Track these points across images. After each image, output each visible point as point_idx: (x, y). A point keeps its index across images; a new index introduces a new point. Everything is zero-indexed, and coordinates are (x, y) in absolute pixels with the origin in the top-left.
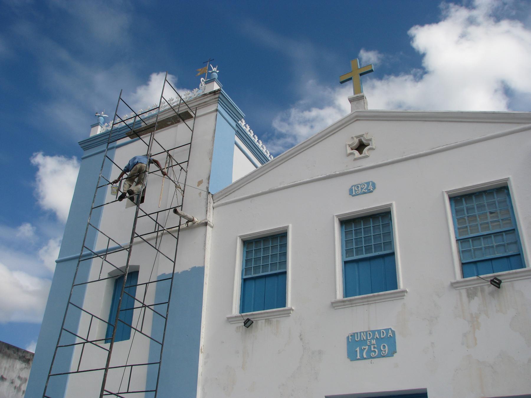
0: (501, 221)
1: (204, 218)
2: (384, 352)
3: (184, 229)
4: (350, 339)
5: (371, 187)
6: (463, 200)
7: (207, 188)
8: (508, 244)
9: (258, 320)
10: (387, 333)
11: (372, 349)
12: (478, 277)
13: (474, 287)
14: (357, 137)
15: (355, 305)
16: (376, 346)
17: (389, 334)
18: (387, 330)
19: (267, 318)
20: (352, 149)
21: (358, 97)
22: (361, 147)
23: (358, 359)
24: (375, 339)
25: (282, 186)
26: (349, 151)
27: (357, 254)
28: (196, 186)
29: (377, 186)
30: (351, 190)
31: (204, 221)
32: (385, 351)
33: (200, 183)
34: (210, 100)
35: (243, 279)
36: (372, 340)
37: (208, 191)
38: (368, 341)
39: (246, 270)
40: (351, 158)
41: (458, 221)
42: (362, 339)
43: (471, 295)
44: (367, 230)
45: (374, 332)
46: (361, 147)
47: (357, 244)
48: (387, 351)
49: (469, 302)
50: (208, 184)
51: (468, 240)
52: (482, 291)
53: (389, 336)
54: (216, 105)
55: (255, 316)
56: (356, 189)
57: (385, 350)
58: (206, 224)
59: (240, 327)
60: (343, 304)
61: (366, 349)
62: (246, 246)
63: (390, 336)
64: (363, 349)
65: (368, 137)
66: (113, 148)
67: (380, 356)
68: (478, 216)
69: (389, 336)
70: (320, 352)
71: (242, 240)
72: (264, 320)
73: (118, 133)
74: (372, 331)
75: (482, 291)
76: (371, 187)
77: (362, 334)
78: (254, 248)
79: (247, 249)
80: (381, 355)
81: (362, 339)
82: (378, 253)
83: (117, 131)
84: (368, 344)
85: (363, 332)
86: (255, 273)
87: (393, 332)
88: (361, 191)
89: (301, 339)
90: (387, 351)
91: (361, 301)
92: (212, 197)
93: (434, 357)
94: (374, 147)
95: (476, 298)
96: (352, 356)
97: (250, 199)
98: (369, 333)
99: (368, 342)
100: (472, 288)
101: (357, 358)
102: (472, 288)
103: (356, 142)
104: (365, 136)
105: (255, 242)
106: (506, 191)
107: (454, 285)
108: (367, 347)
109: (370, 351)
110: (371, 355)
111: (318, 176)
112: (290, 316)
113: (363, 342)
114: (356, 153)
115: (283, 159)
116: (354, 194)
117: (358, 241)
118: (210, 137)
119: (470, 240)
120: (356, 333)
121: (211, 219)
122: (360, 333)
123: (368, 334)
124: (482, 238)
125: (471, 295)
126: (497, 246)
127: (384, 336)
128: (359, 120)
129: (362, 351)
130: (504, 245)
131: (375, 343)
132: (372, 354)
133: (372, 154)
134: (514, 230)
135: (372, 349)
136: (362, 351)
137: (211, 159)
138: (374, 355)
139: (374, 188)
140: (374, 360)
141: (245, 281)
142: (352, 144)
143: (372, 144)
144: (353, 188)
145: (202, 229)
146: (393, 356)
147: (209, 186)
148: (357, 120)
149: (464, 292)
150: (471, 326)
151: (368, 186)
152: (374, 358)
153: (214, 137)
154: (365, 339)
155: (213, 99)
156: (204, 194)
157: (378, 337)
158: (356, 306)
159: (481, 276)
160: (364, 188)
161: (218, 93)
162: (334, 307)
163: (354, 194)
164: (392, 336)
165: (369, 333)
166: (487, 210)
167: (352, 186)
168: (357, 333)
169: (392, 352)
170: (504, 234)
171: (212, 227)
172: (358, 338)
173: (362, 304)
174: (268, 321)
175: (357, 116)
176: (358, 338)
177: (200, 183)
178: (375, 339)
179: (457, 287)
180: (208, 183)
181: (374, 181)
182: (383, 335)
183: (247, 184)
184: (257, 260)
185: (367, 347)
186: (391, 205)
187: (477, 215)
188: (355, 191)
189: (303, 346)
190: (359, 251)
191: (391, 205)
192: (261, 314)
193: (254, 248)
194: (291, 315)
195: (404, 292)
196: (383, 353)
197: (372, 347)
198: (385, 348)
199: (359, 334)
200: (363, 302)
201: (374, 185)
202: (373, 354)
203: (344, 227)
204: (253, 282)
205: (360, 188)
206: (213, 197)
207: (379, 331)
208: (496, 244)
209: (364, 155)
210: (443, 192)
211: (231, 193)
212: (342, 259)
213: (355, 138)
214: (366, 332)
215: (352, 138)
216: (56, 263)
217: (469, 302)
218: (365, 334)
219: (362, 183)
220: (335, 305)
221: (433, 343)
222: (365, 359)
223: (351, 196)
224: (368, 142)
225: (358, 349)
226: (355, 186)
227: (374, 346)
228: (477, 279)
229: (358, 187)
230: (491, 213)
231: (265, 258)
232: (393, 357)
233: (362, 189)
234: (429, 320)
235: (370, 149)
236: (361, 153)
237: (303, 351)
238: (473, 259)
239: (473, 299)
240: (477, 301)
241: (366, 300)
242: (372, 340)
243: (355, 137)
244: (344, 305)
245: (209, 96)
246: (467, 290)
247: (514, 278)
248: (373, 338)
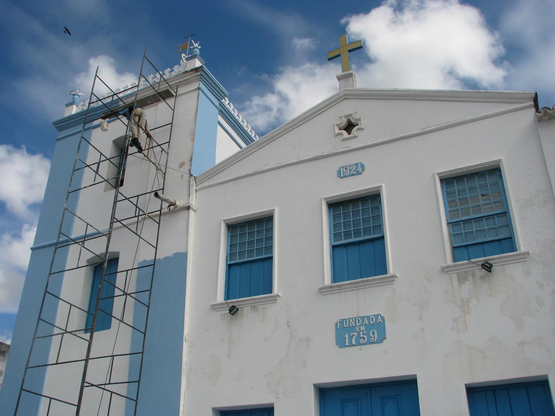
0: (492, 204)
1: (186, 202)
2: (373, 339)
3: (166, 213)
4: (338, 326)
5: (360, 169)
7: (190, 171)
8: (499, 227)
9: (244, 307)
10: (377, 319)
11: (362, 336)
12: (469, 261)
13: (465, 272)
14: (345, 117)
15: (343, 291)
16: (365, 332)
17: (379, 320)
18: (376, 316)
19: (253, 305)
20: (340, 129)
21: (346, 74)
22: (349, 127)
23: (347, 346)
24: (364, 325)
25: (268, 168)
26: (337, 131)
27: (345, 238)
28: (178, 169)
29: (366, 168)
30: (339, 172)
31: (186, 205)
32: (374, 337)
33: (182, 165)
34: (192, 78)
35: (228, 265)
36: (361, 327)
38: (357, 327)
39: (231, 255)
40: (340, 138)
41: (449, 204)
42: (351, 326)
43: (462, 280)
44: (356, 214)
45: (363, 318)
46: (349, 127)
47: (345, 227)
48: (376, 338)
49: (460, 286)
51: (459, 223)
52: (473, 275)
53: (378, 322)
54: (199, 82)
55: (240, 303)
56: (344, 171)
57: (374, 336)
58: (188, 208)
59: (225, 314)
60: (330, 289)
61: (354, 335)
62: (230, 231)
63: (379, 321)
64: (352, 335)
65: (356, 117)
66: (89, 128)
67: (370, 343)
68: (470, 198)
69: (378, 322)
70: (308, 339)
71: (226, 224)
72: (250, 307)
73: (94, 113)
74: (361, 317)
75: (473, 275)
76: (360, 169)
77: (351, 320)
78: (239, 233)
79: (232, 233)
80: (371, 342)
81: (351, 326)
82: (367, 236)
83: (94, 111)
84: (357, 331)
85: (352, 319)
87: (383, 318)
88: (350, 172)
89: (288, 326)
90: (376, 338)
91: (350, 286)
92: (195, 179)
93: (424, 343)
94: (363, 127)
95: (466, 282)
96: (341, 343)
97: (234, 182)
98: (358, 319)
99: (357, 329)
100: (463, 273)
101: (346, 345)
102: (463, 273)
103: (344, 121)
104: (354, 115)
105: (240, 226)
106: (498, 173)
107: (445, 270)
108: (356, 334)
109: (359, 337)
110: (360, 342)
111: (305, 157)
112: (277, 302)
113: (352, 329)
114: (345, 133)
115: (268, 140)
116: (342, 175)
117: (346, 225)
118: (192, 117)
119: (462, 223)
120: (344, 319)
121: (193, 202)
122: (349, 319)
123: (357, 320)
124: (473, 221)
125: (462, 280)
126: (488, 229)
127: (373, 323)
128: (348, 99)
129: (351, 337)
130: (495, 229)
131: (364, 330)
132: (361, 341)
133: (360, 134)
134: (506, 212)
135: (362, 336)
136: (351, 337)
137: (193, 140)
138: (363, 342)
139: (363, 169)
140: (363, 347)
141: (229, 267)
142: (340, 123)
143: (361, 123)
144: (342, 169)
145: (185, 213)
146: (383, 342)
147: (191, 168)
148: (346, 99)
149: (454, 277)
150: (461, 311)
151: (357, 167)
152: (363, 344)
153: (196, 116)
154: (354, 325)
155: (194, 77)
156: (186, 176)
157: (367, 323)
158: (345, 291)
159: (472, 260)
160: (353, 169)
161: (200, 71)
162: (322, 293)
163: (342, 175)
164: (381, 322)
166: (479, 193)
167: (340, 168)
168: (346, 320)
169: (382, 339)
170: (496, 217)
171: (195, 211)
172: (346, 325)
173: (351, 289)
174: (254, 308)
175: (345, 95)
176: (346, 325)
177: (182, 165)
178: (364, 325)
179: (448, 272)
180: (191, 165)
181: (362, 162)
182: (372, 321)
183: (231, 165)
184: (242, 244)
185: (356, 334)
186: (380, 187)
187: (469, 198)
188: (344, 172)
189: (290, 333)
190: (347, 235)
191: (380, 187)
192: (247, 300)
193: (239, 233)
194: (277, 301)
195: (394, 276)
196: (372, 339)
197: (361, 333)
198: (375, 334)
199: (348, 320)
200: (352, 288)
202: (363, 340)
203: (332, 210)
204: (239, 268)
205: (348, 169)
206: (196, 180)
207: (368, 317)
208: (487, 228)
209: (353, 135)
210: (434, 173)
211: (214, 175)
212: (330, 243)
213: (343, 118)
214: (355, 318)
215: (341, 117)
216: (31, 251)
217: (460, 286)
218: (354, 320)
219: (351, 164)
220: (323, 290)
221: (423, 329)
222: (354, 345)
223: (339, 178)
224: (357, 122)
225: (347, 336)
226: (343, 167)
227: (363, 332)
228: (468, 263)
229: (346, 169)
230: (483, 195)
231: (251, 243)
232: (382, 344)
233: (350, 170)
234: (419, 306)
235: (359, 129)
236: (349, 133)
237: (291, 338)
238: (464, 242)
239: (464, 283)
240: (467, 286)
241: (354, 285)
242: (361, 327)
243: (343, 116)
244: (332, 291)
245: (191, 73)
246: (458, 274)
247: (505, 262)
248: (362, 325)
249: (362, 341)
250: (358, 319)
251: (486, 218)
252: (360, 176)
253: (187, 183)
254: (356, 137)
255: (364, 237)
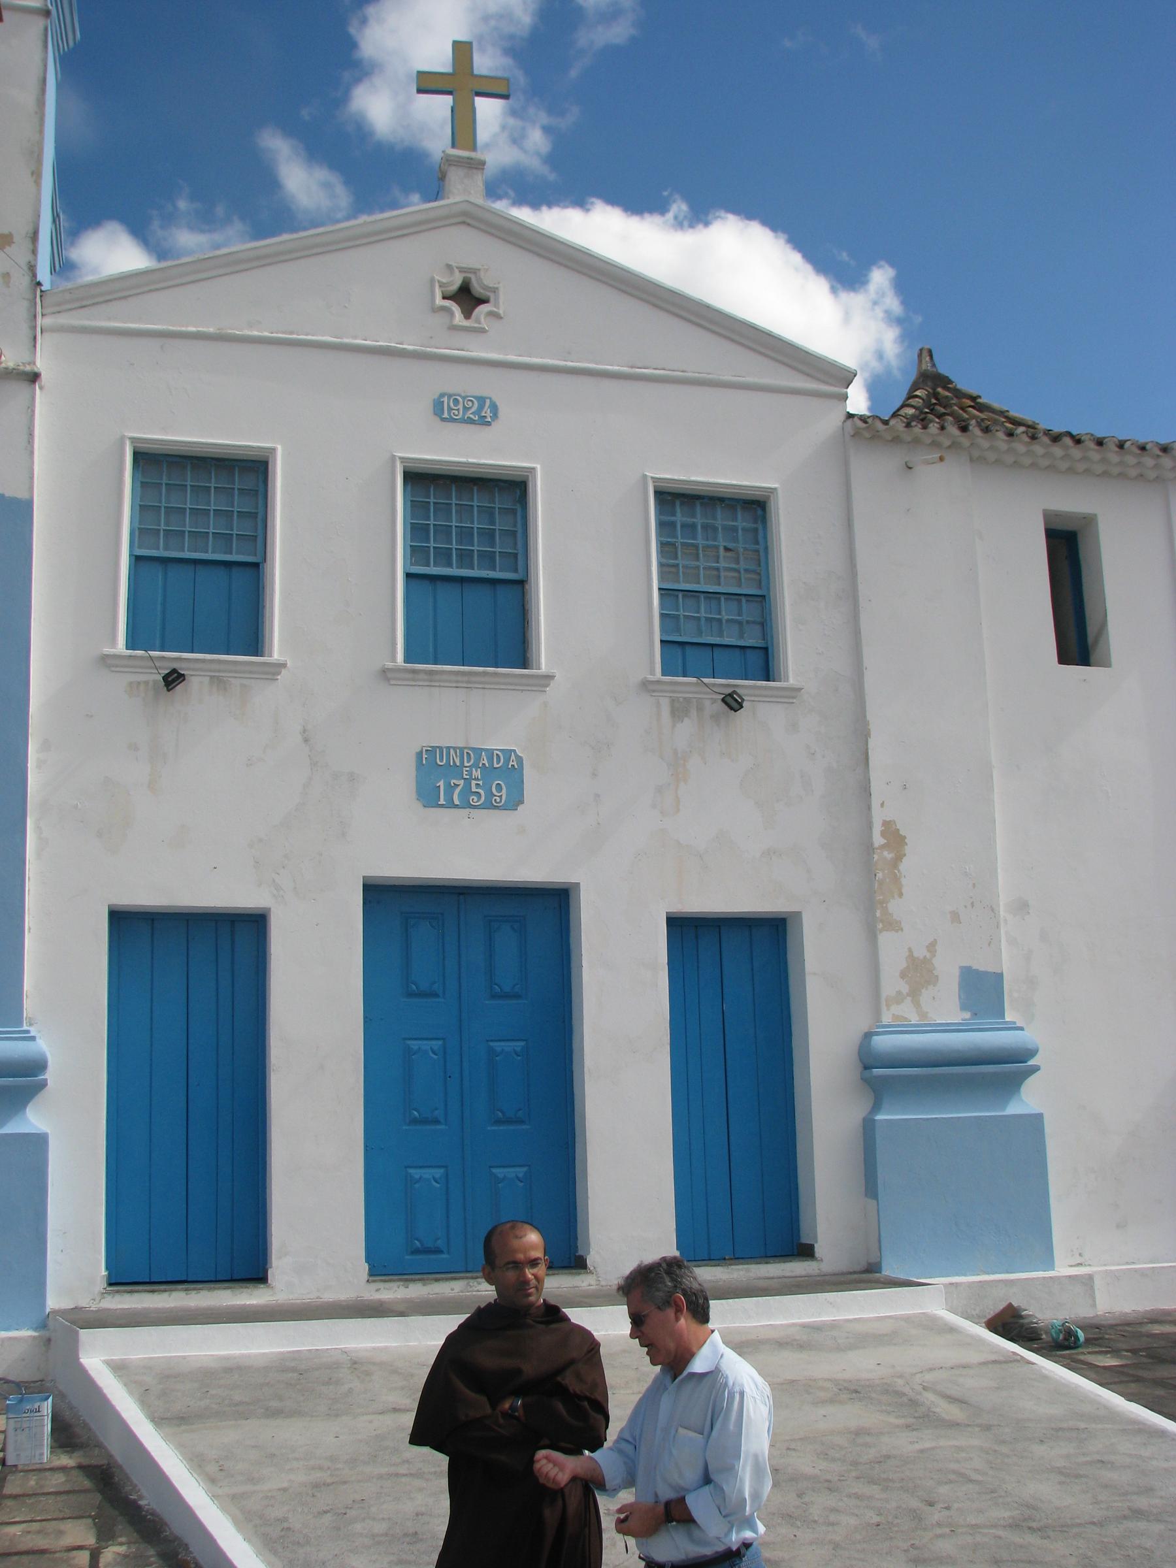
0: (742, 572)
1: (27, 359)
2: (498, 800)
4: (424, 759)
6: (678, 503)
8: (748, 622)
9: (192, 675)
10: (508, 760)
11: (474, 789)
12: (699, 681)
13: (685, 698)
14: (462, 270)
15: (437, 684)
16: (480, 783)
17: (511, 763)
18: (508, 753)
19: (217, 674)
20: (444, 298)
21: (472, 159)
23: (442, 806)
24: (479, 768)
26: (439, 301)
29: (501, 414)
32: (501, 797)
35: (134, 557)
36: (474, 769)
37: (34, 275)
38: (464, 769)
39: (140, 533)
41: (661, 547)
42: (452, 764)
43: (679, 711)
45: (478, 751)
47: (482, 554)
48: (504, 798)
49: (674, 726)
50: (30, 257)
51: (676, 593)
52: (700, 709)
53: (510, 766)
55: (184, 665)
56: (452, 405)
57: (499, 794)
59: (139, 683)
60: (410, 676)
61: (459, 785)
62: (141, 468)
63: (513, 766)
64: (453, 785)
65: (488, 281)
67: (489, 805)
68: (703, 547)
69: (510, 766)
70: (352, 777)
72: (208, 678)
74: (473, 749)
75: (700, 709)
77: (452, 751)
80: (469, 801)
81: (452, 764)
82: (488, 572)
84: (465, 777)
85: (455, 749)
86: (166, 548)
87: (520, 760)
88: (464, 414)
89: (306, 740)
90: (504, 798)
91: (453, 678)
92: (41, 296)
93: (599, 824)
95: (686, 720)
96: (428, 796)
98: (467, 753)
99: (465, 773)
100: (681, 700)
101: (439, 803)
102: (681, 700)
103: (456, 282)
106: (760, 512)
107: (646, 686)
108: (462, 782)
109: (467, 792)
110: (494, 802)
111: (355, 337)
112: (277, 679)
113: (456, 771)
114: (456, 309)
115: (258, 258)
116: (446, 415)
119: (680, 595)
120: (437, 747)
122: (448, 748)
123: (465, 754)
124: (702, 596)
125: (679, 711)
126: (728, 621)
127: (498, 766)
128: (469, 225)
129: (450, 789)
130: (740, 623)
131: (479, 777)
132: (473, 799)
134: (763, 597)
135: (474, 789)
136: (450, 789)
138: (477, 802)
140: (474, 812)
142: (448, 283)
143: (497, 300)
146: (517, 809)
147: (36, 260)
148: (464, 223)
149: (665, 704)
150: (672, 775)
151: (481, 407)
152: (475, 807)
154: (458, 764)
156: (21, 281)
157: (487, 765)
158: (440, 686)
159: (705, 680)
160: (470, 408)
162: (388, 680)
163: (446, 415)
164: (516, 767)
165: (497, 754)
166: (721, 542)
167: (442, 395)
168: (441, 748)
169: (515, 801)
170: (744, 600)
171: (41, 388)
172: (441, 760)
173: (454, 685)
174: (219, 682)
175: (465, 214)
176: (441, 760)
178: (479, 768)
179: (654, 691)
181: (494, 399)
182: (498, 762)
183: (150, 291)
185: (462, 782)
187: (700, 546)
188: (450, 409)
189: (309, 756)
190: (444, 556)
192: (203, 661)
194: (279, 677)
195: (550, 677)
196: (495, 800)
197: (474, 783)
198: (501, 790)
199: (444, 750)
200: (457, 682)
201: (495, 409)
202: (476, 799)
203: (409, 488)
205: (461, 407)
206: (42, 298)
207: (490, 753)
208: (726, 617)
209: (476, 325)
210: (645, 477)
211: (97, 303)
213: (457, 271)
214: (462, 749)
215: (449, 267)
217: (674, 726)
218: (458, 754)
219: (469, 394)
220: (385, 674)
221: (597, 796)
222: (456, 806)
223: (438, 419)
224: (488, 294)
225: (441, 784)
226: (450, 396)
227: (479, 783)
228: (697, 684)
229: (456, 402)
230: (727, 549)
232: (516, 812)
233: (466, 409)
234: (593, 748)
235: (492, 314)
236: (468, 314)
237: (311, 769)
238: (681, 636)
239: (682, 722)
240: (686, 728)
241: (465, 679)
242: (474, 769)
243: (457, 268)
244: (413, 680)
246: (673, 701)
247: (760, 696)
248: (476, 766)
249: (474, 801)
250: (467, 753)
251: (726, 596)
252: (487, 428)
253: (26, 304)
254: (483, 331)
255: (479, 571)
